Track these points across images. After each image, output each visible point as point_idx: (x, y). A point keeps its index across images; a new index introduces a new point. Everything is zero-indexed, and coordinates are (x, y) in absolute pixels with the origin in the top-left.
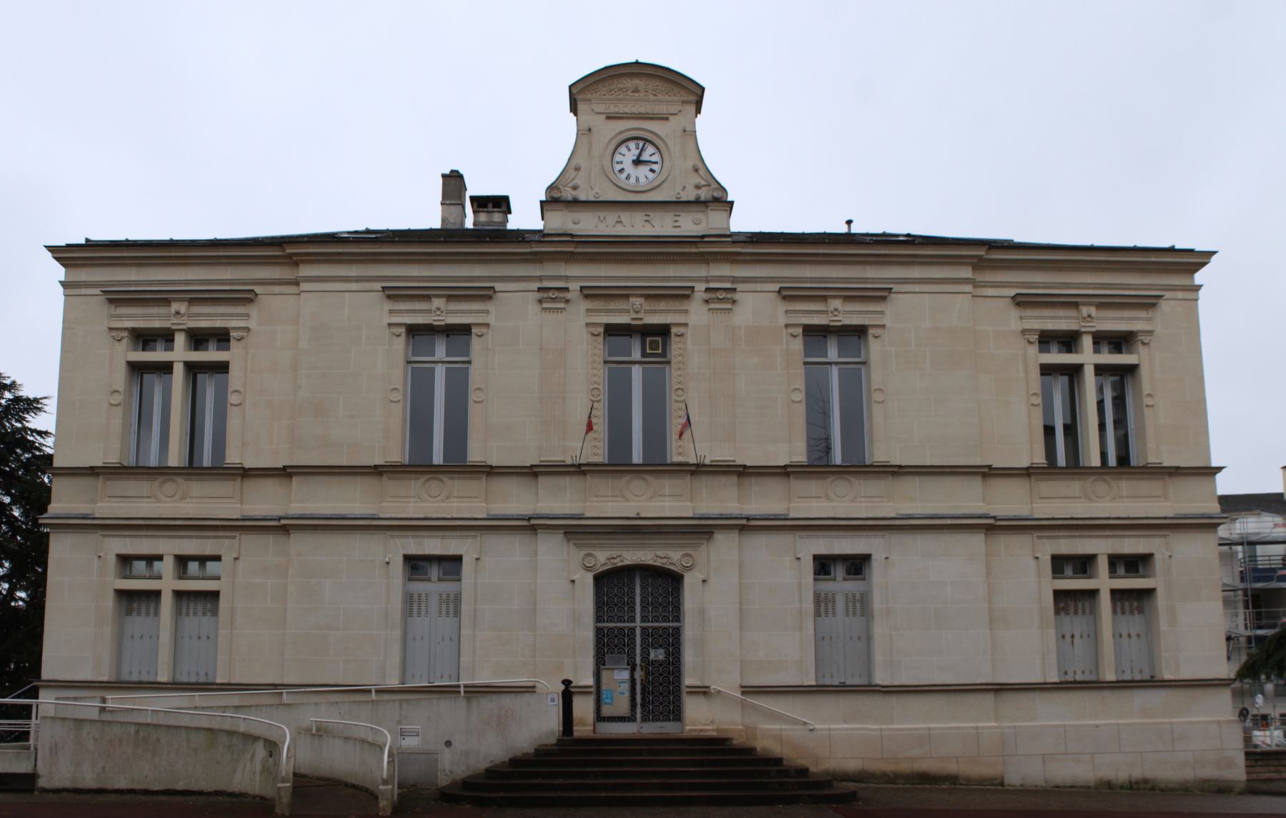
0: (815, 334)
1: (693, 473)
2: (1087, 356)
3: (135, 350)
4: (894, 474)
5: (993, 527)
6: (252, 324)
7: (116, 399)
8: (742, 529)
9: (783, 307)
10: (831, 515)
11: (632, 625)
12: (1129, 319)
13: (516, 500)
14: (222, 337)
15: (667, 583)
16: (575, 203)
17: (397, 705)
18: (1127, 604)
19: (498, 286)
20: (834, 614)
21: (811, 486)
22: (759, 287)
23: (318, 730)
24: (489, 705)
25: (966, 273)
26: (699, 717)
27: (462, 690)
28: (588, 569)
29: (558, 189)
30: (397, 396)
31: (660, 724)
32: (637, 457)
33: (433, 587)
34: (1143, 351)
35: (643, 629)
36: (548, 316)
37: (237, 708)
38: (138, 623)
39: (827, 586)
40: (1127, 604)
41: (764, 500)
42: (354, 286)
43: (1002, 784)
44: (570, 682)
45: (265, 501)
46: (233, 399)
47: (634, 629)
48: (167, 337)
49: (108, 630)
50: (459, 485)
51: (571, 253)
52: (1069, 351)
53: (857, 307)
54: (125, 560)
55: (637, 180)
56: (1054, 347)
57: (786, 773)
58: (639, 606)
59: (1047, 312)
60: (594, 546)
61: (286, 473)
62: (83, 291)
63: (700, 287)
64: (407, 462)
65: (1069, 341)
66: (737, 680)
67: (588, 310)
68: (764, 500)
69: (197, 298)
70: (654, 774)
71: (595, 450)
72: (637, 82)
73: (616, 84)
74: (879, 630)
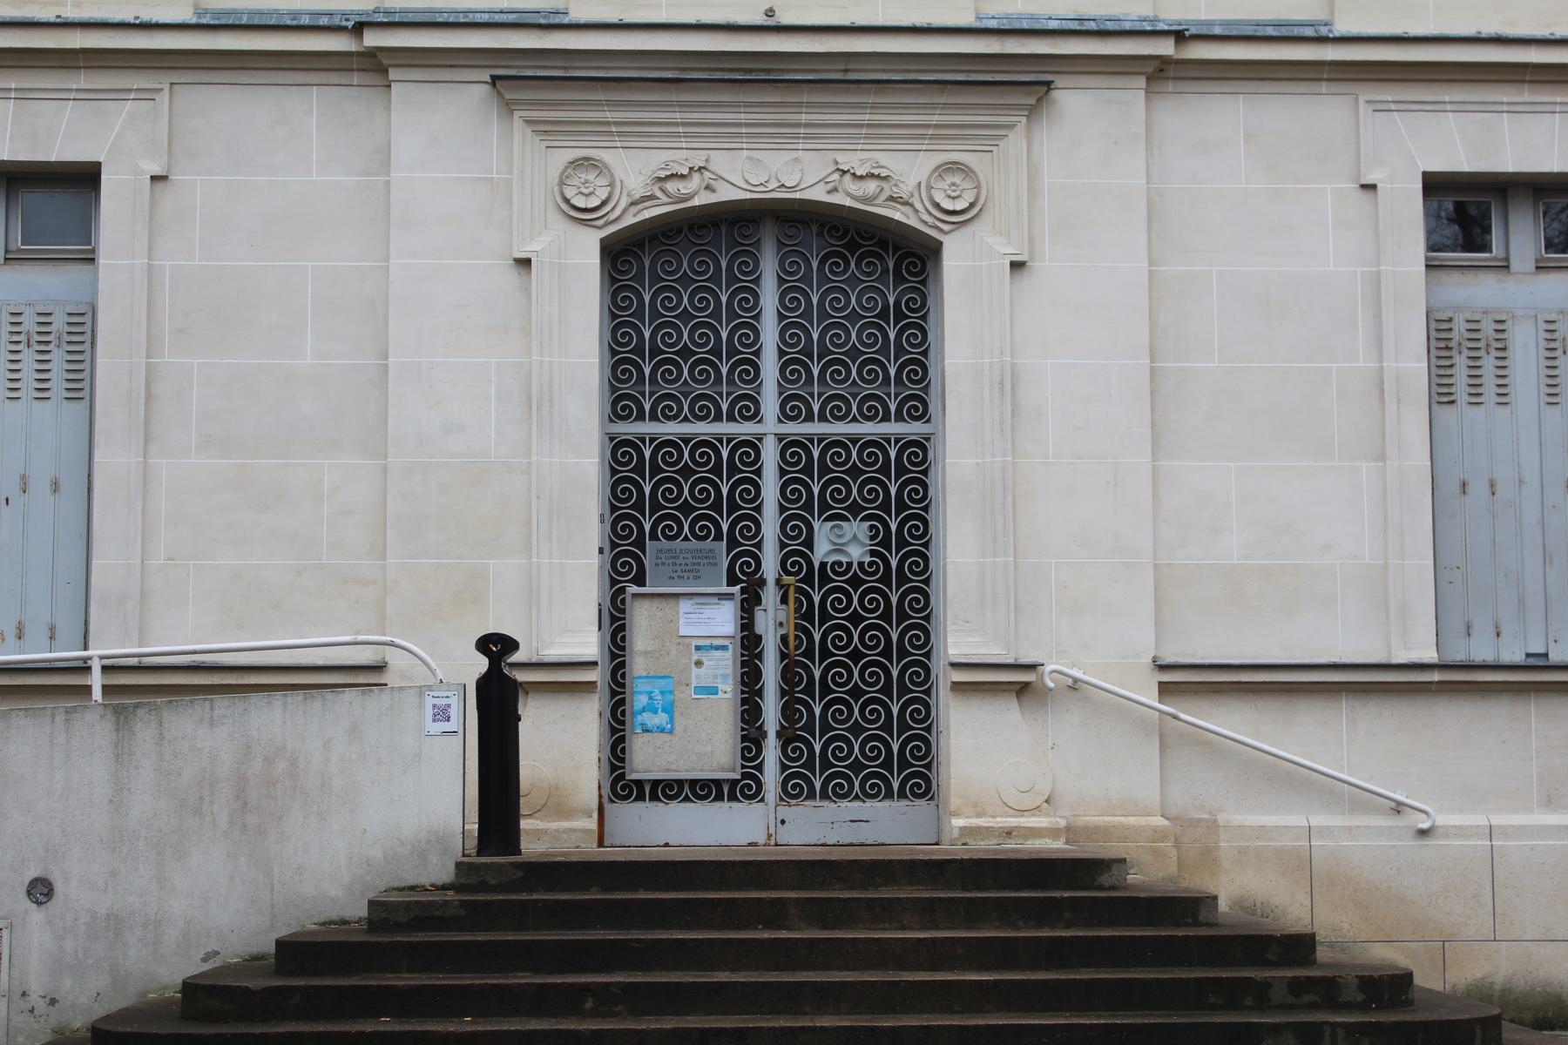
8: (1159, 72)
10: (1488, 30)
15: (880, 266)
24: (203, 736)
26: (1001, 782)
27: (96, 680)
28: (582, 216)
31: (850, 808)
35: (788, 445)
39: (1475, 292)
44: (509, 644)
47: (753, 445)
57: (1328, 990)
60: (602, 129)
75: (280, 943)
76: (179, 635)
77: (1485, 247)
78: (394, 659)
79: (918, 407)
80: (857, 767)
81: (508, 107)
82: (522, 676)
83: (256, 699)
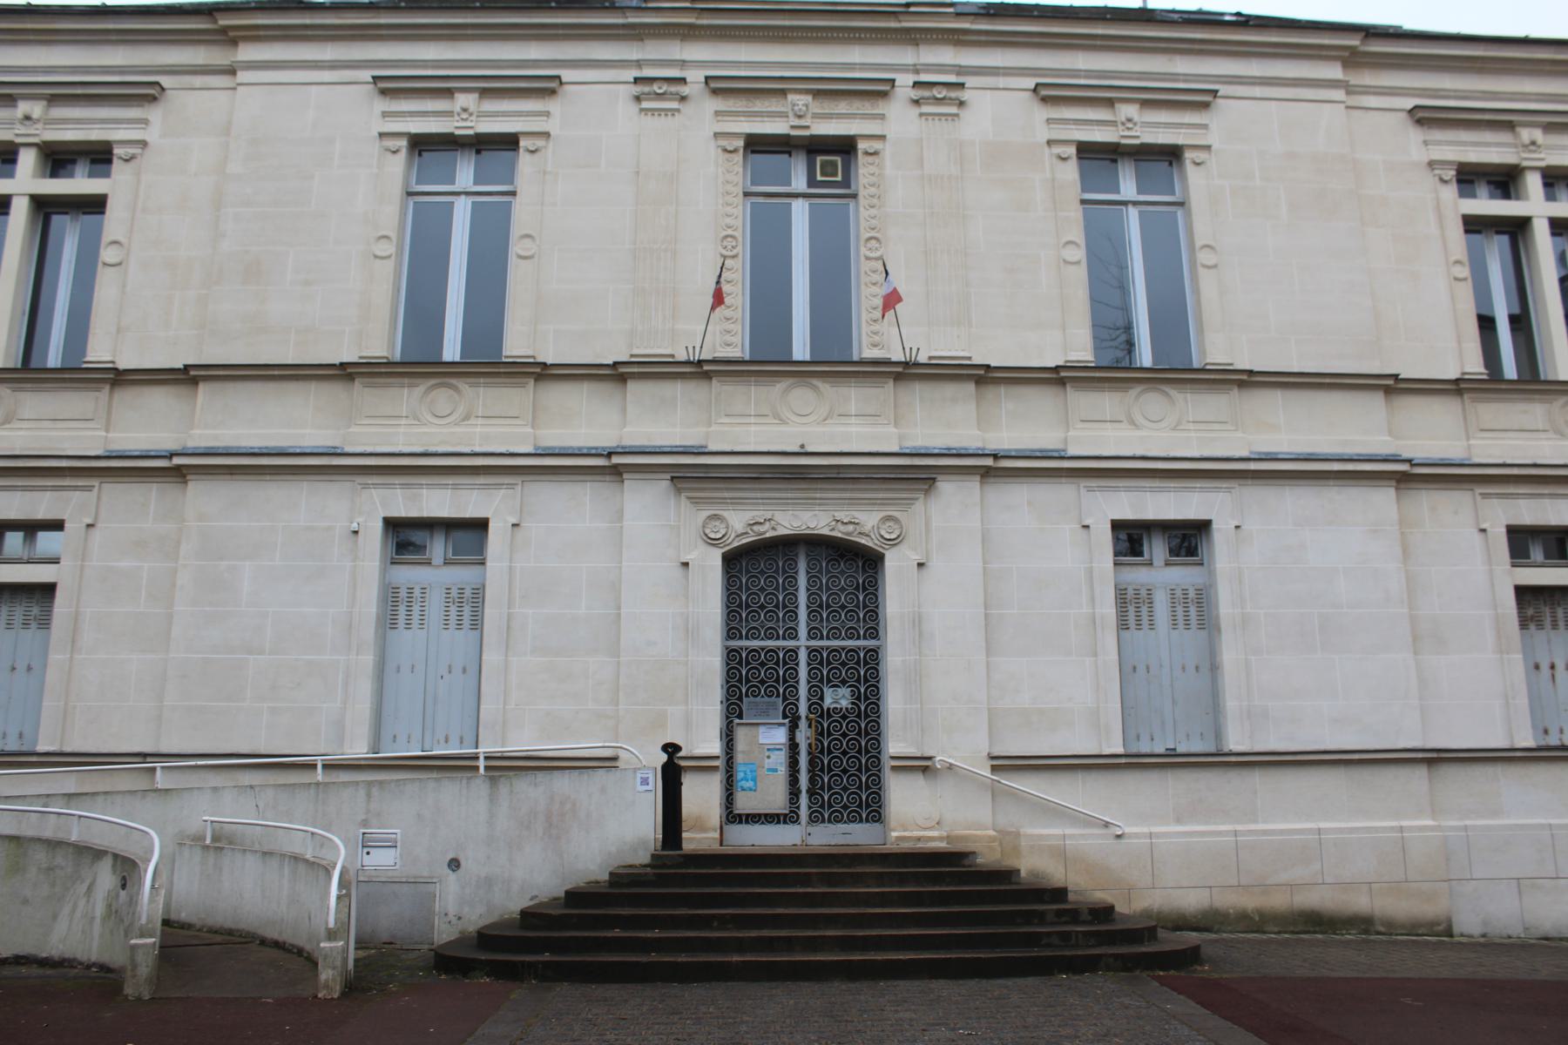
1: (898, 377)
4: (1241, 384)
5: (1408, 477)
8: (986, 474)
9: (1042, 113)
10: (1139, 453)
11: (791, 643)
13: (586, 420)
14: (100, 156)
15: (855, 565)
17: (362, 792)
19: (567, 75)
20: (1152, 625)
21: (1105, 402)
22: (1002, 82)
23: (215, 838)
24: (531, 792)
25: (1334, 71)
26: (915, 815)
27: (482, 763)
28: (713, 542)
30: (387, 248)
31: (841, 827)
32: (801, 349)
33: (434, 575)
36: (649, 121)
37: (70, 796)
39: (1137, 576)
41: (1022, 425)
42: (327, 76)
44: (677, 748)
45: (148, 424)
46: (108, 254)
47: (795, 651)
51: (691, 26)
52: (1507, 195)
56: (1483, 190)
57: (1074, 915)
58: (802, 613)
61: (187, 377)
63: (905, 80)
64: (397, 357)
65: (1505, 180)
67: (717, 113)
68: (1022, 425)
71: (728, 338)
74: (1230, 655)
75: (567, 892)
76: (521, 742)
77: (1140, 554)
78: (622, 754)
79: (874, 633)
80: (845, 807)
82: (683, 763)
83: (556, 773)
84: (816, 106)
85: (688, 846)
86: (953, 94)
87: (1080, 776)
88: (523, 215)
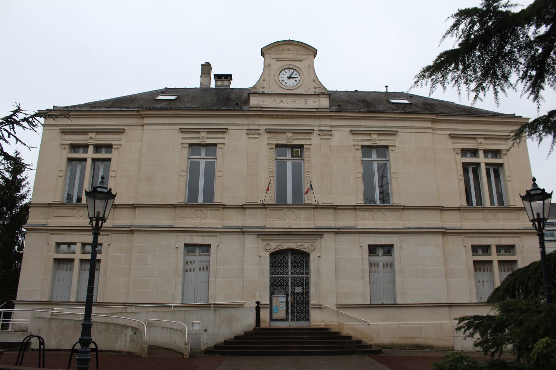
0: (366, 149)
1: (314, 208)
2: (482, 159)
3: (70, 153)
4: (402, 209)
5: (445, 233)
6: (122, 142)
7: (61, 174)
8: (336, 233)
9: (352, 137)
10: (375, 227)
12: (498, 144)
13: (235, 219)
14: (109, 147)
15: (302, 258)
16: (263, 94)
18: (506, 267)
19: (229, 127)
20: (378, 271)
22: (342, 129)
25: (429, 124)
26: (317, 319)
28: (267, 251)
29: (256, 88)
30: (184, 174)
33: (197, 258)
34: (505, 157)
35: (292, 278)
36: (250, 140)
38: (62, 274)
39: (374, 259)
40: (506, 267)
41: (346, 220)
42: (167, 127)
43: (453, 350)
47: (288, 278)
48: (85, 147)
49: (49, 277)
50: (208, 213)
53: (384, 138)
54: (58, 244)
55: (290, 84)
59: (463, 141)
60: (270, 240)
61: (133, 207)
62: (51, 128)
63: (316, 129)
65: (474, 153)
66: (335, 302)
68: (346, 220)
69: (99, 132)
70: (296, 343)
71: (271, 198)
72: (289, 47)
73: (281, 48)
74: (398, 279)
79: (308, 273)
81: (259, 238)
84: (294, 136)
85: (261, 327)
86: (329, 133)
87: (359, 309)
88: (219, 165)
